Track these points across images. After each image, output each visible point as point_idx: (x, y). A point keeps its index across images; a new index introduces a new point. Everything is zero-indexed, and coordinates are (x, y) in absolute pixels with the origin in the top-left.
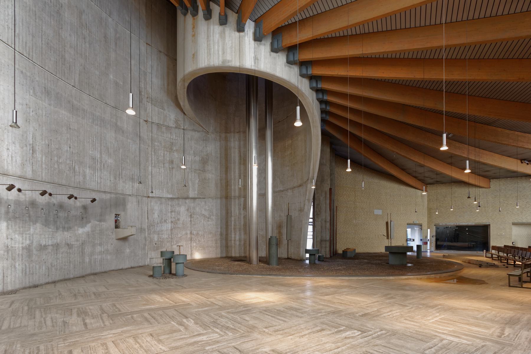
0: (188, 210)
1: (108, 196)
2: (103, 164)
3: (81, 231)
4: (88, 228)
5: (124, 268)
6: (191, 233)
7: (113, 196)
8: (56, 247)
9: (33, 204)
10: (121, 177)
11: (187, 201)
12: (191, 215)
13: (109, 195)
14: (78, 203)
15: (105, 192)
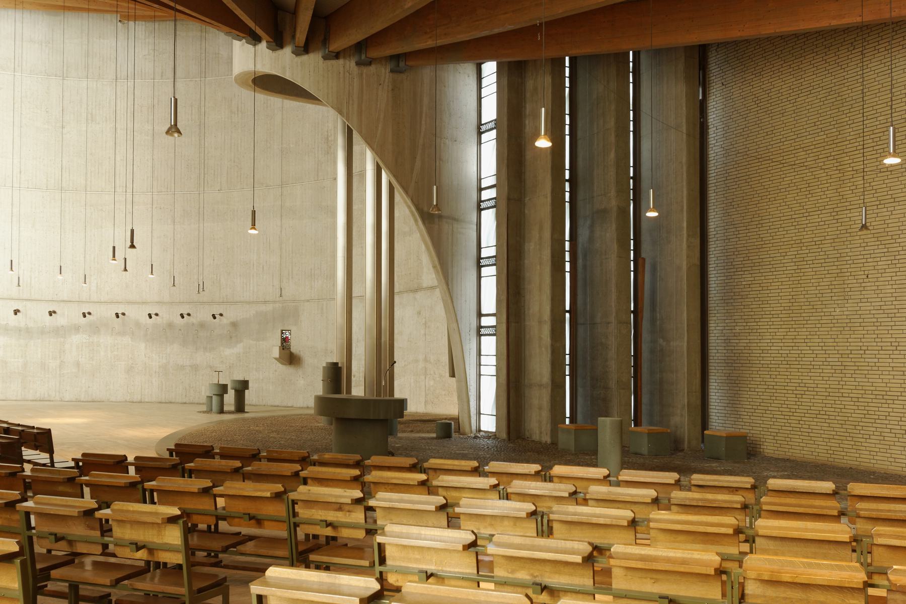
0: (419, 313)
1: (270, 307)
2: (261, 267)
3: (228, 352)
4: (238, 349)
5: (295, 406)
6: (426, 360)
7: (277, 305)
8: (195, 368)
9: (170, 325)
10: (291, 277)
11: (419, 295)
12: (425, 323)
13: (271, 305)
14: (224, 320)
15: (265, 302)
